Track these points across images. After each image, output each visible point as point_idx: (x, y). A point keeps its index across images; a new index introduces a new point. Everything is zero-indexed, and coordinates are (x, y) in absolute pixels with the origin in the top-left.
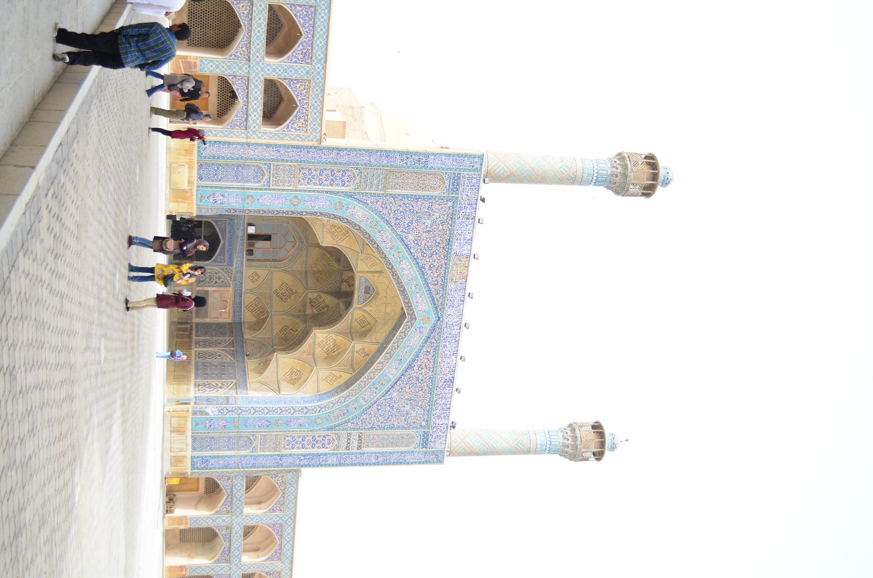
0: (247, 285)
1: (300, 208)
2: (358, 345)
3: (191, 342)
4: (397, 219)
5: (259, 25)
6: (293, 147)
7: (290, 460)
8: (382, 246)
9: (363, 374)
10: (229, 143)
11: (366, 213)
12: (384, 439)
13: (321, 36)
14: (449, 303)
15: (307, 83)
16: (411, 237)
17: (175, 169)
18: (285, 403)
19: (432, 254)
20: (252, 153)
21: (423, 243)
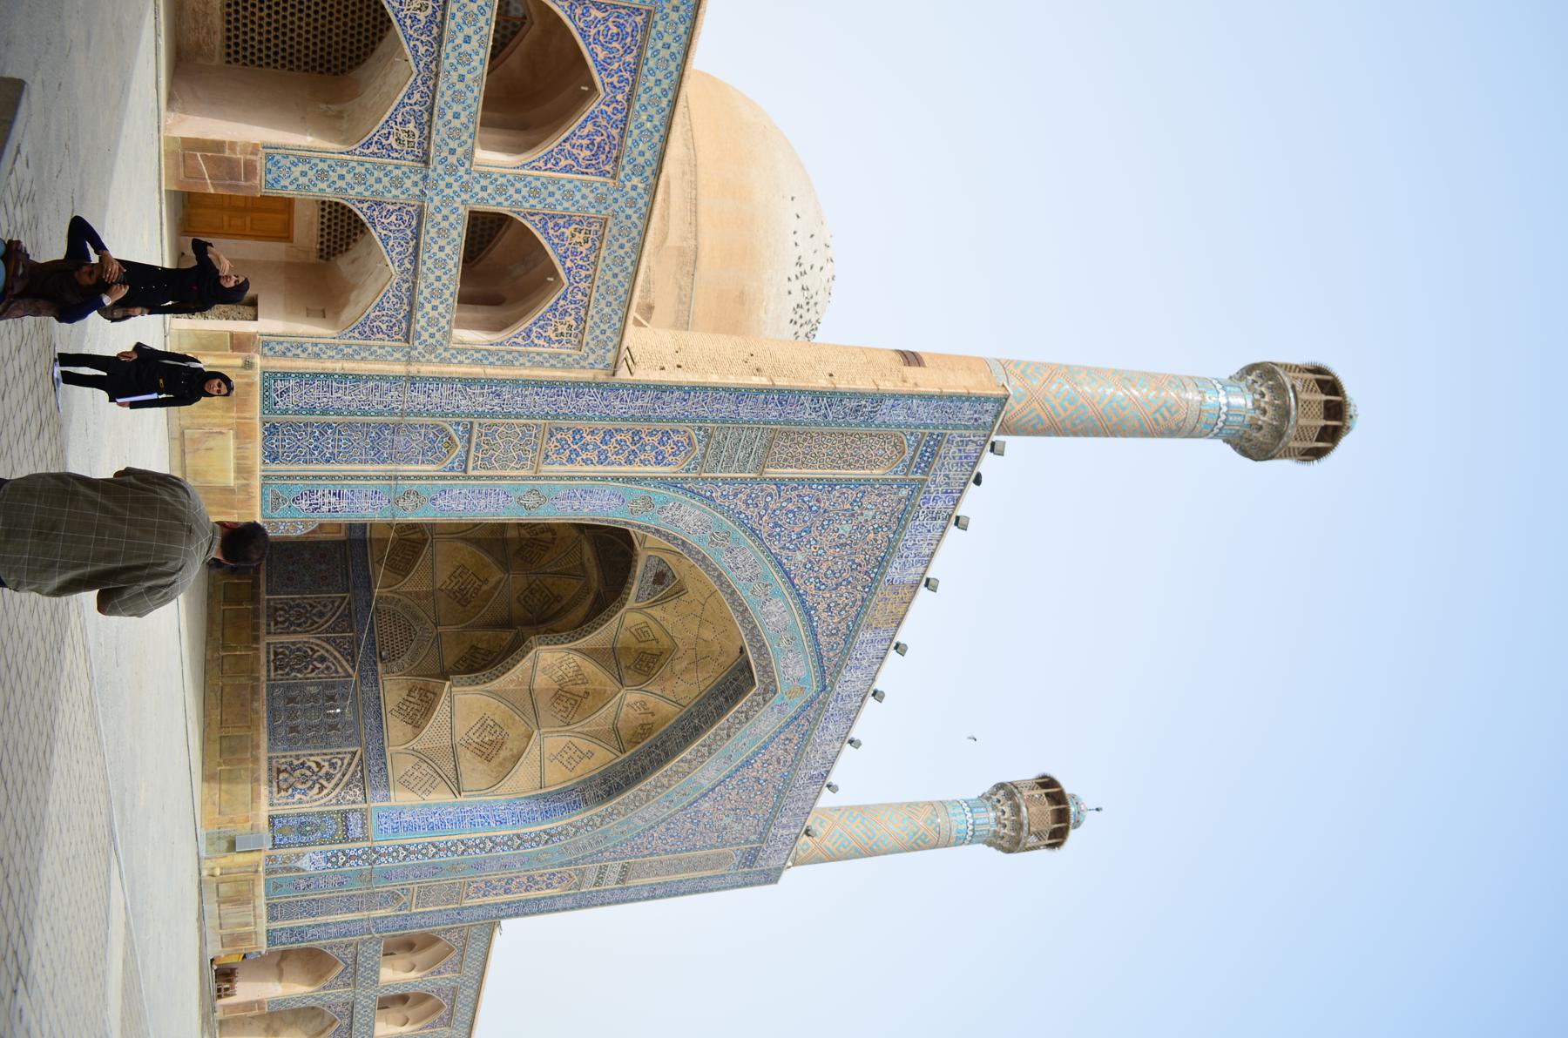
3: (256, 613)
4: (776, 525)
5: (465, 59)
6: (539, 383)
7: (481, 912)
8: (730, 576)
10: (358, 378)
11: (706, 517)
13: (654, 101)
15: (596, 230)
16: (800, 557)
17: (193, 440)
20: (422, 398)
21: (824, 567)
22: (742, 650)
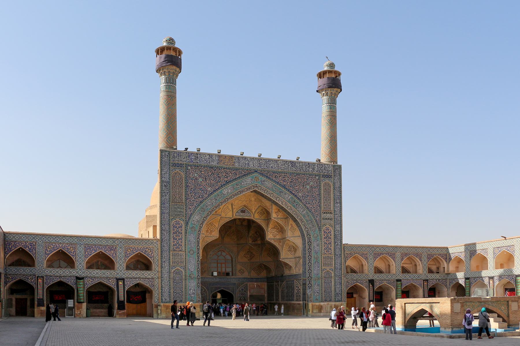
0: (246, 275)
1: (195, 250)
2: (274, 216)
4: (199, 197)
5: (97, 273)
6: (161, 254)
9: (289, 212)
12: (326, 200)
14: (247, 166)
18: (306, 254)
19: (219, 177)
20: (166, 275)
22: (251, 192)
